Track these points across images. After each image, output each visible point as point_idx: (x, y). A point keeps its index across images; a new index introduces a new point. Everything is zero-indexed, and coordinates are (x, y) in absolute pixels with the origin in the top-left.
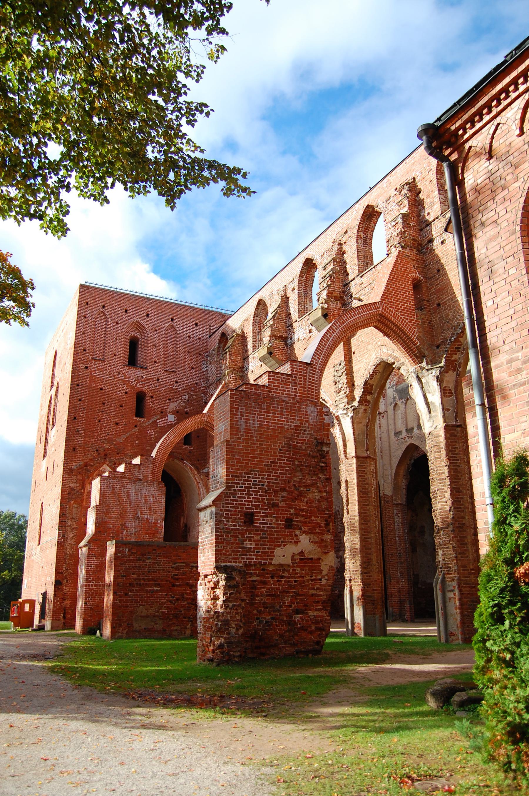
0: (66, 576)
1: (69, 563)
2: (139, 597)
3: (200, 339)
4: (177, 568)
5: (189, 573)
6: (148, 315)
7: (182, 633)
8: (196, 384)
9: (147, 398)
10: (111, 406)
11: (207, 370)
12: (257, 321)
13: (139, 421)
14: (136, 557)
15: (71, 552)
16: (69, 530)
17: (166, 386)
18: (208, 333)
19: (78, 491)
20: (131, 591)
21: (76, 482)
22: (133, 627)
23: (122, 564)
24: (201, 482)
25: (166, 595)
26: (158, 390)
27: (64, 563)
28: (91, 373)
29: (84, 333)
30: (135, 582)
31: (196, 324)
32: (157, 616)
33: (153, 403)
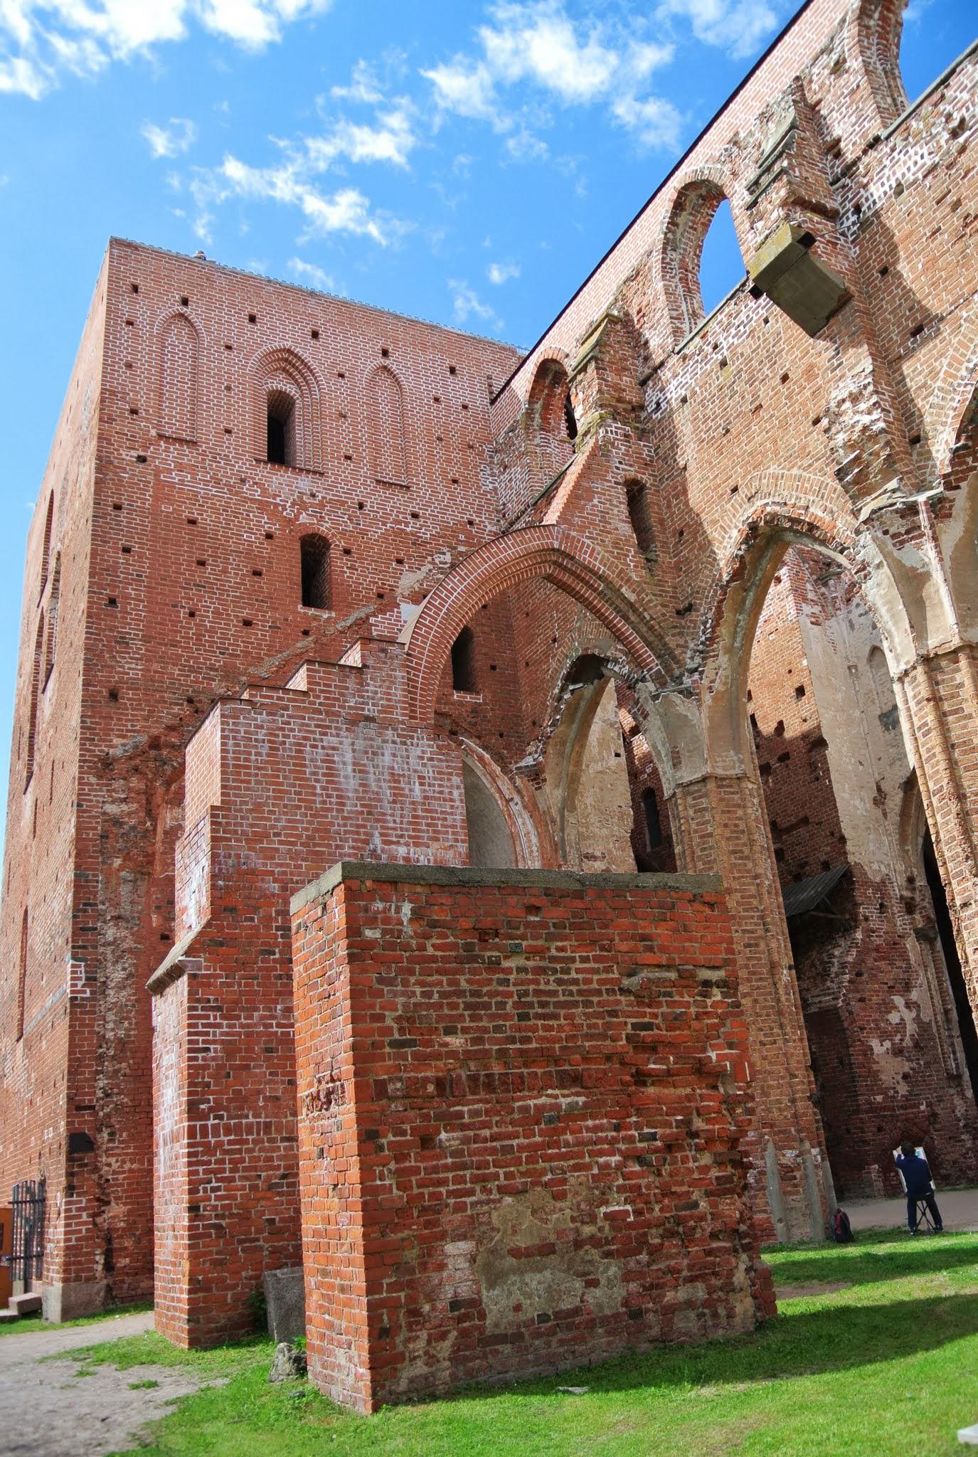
0: (108, 1116)
1: (116, 1072)
2: (493, 1151)
3: (465, 407)
4: (645, 997)
5: (698, 1017)
6: (315, 335)
7: (715, 1315)
8: (471, 523)
9: (334, 553)
10: (225, 571)
11: (495, 489)
12: (675, 264)
13: (316, 618)
14: (454, 946)
15: (121, 1033)
16: (110, 956)
17: (384, 524)
18: (486, 394)
19: (133, 828)
20: (452, 1121)
21: (124, 800)
22: (482, 1316)
23: (390, 982)
24: (517, 798)
25: (617, 1128)
26: (363, 533)
27: (97, 1072)
28: (157, 475)
29: (129, 366)
30: (463, 1074)
31: (453, 370)
32: (594, 1242)
33: (352, 568)
